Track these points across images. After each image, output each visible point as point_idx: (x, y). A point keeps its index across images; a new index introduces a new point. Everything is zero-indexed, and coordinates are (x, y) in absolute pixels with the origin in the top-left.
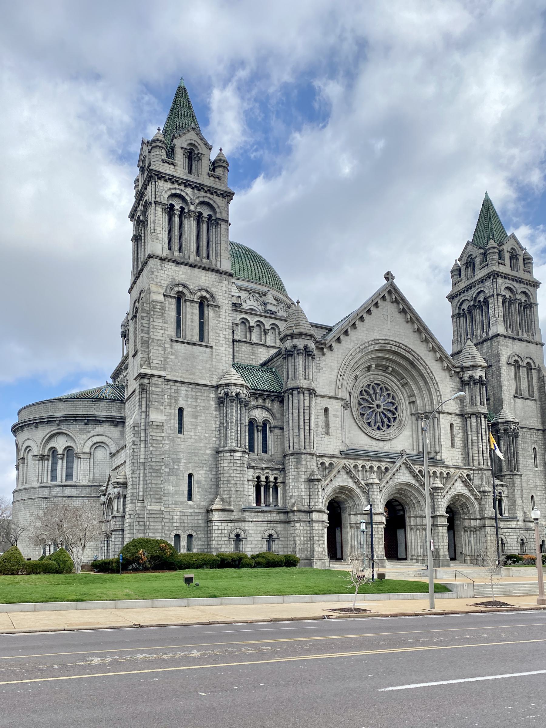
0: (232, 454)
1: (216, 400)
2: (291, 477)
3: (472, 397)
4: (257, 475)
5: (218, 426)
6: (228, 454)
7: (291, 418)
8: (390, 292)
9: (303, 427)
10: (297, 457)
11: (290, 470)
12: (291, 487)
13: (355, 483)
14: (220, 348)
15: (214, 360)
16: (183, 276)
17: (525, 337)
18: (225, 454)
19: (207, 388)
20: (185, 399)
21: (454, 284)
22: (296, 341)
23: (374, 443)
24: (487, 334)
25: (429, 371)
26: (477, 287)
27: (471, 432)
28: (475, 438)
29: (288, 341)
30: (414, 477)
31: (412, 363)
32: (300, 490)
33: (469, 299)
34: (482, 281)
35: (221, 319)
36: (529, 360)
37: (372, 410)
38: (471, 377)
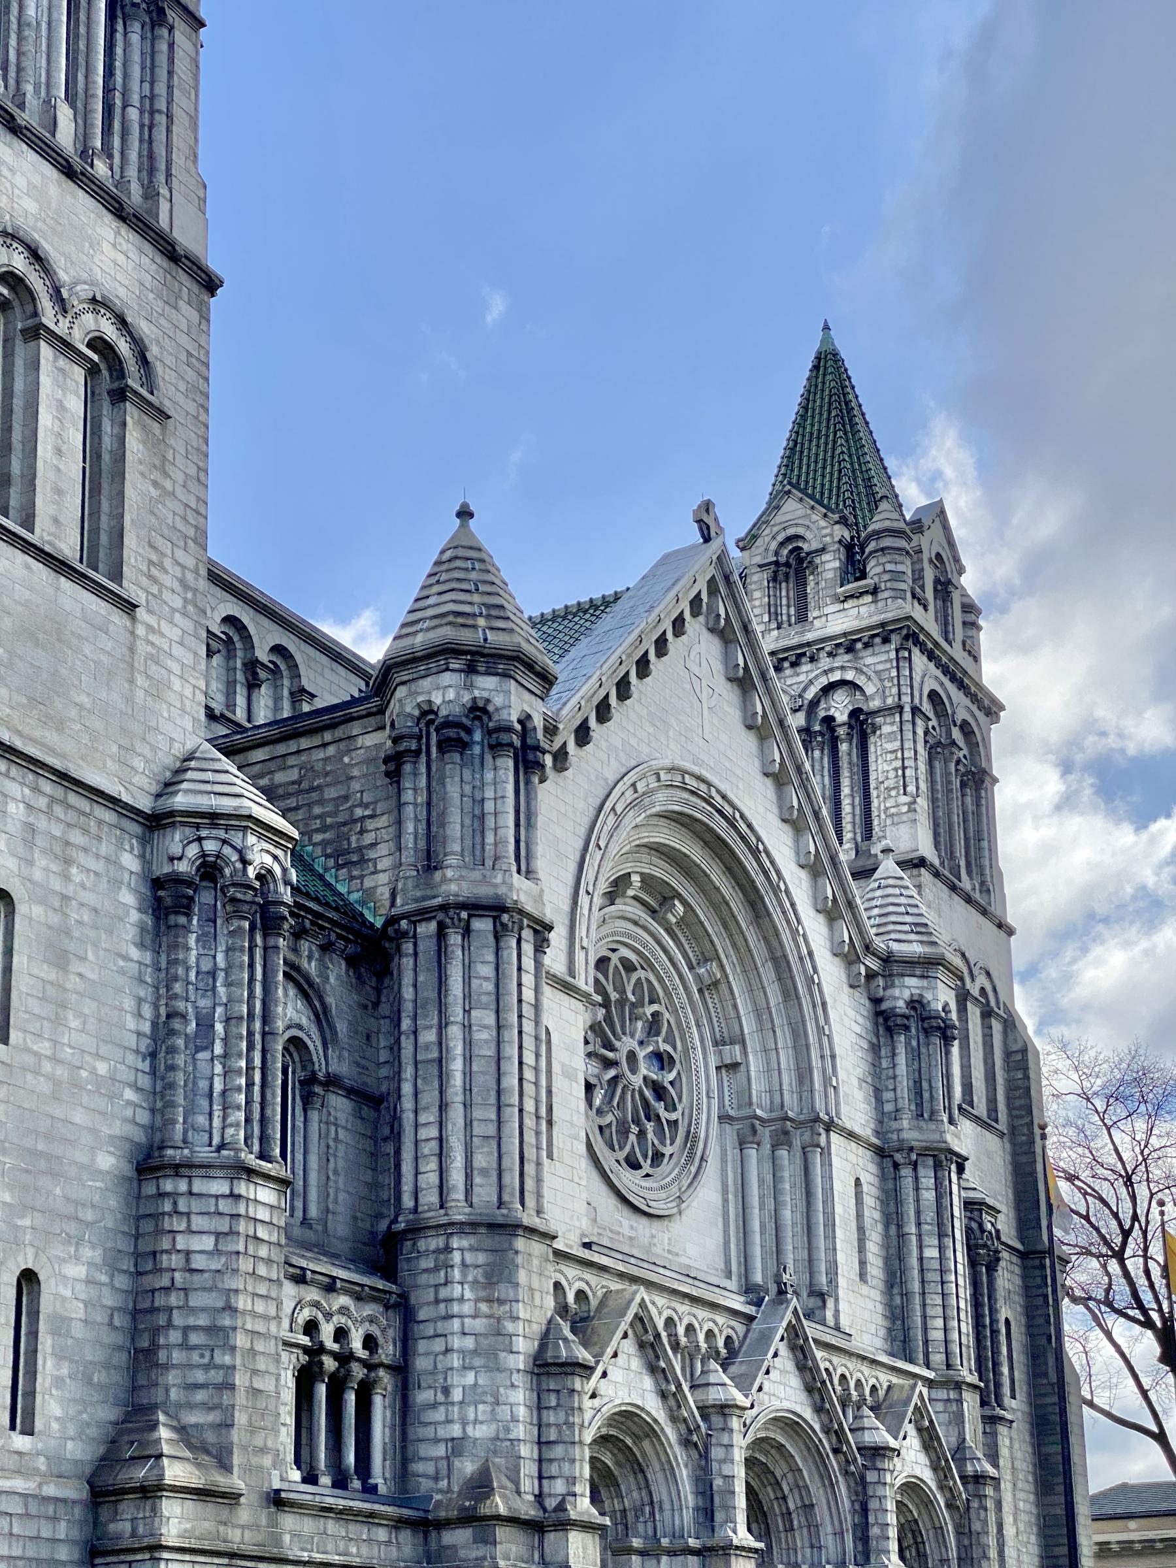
0: (242, 1188)
1: (145, 890)
2: (456, 1342)
4: (305, 1315)
5: (146, 1028)
6: (220, 1187)
7: (457, 1048)
9: (515, 1100)
10: (488, 1241)
11: (456, 1308)
12: (457, 1395)
13: (663, 1395)
14: (165, 628)
15: (140, 680)
16: (31, 206)
18: (198, 1186)
19: (109, 816)
20: (20, 850)
22: (486, 685)
23: (626, 1222)
25: (804, 951)
27: (919, 1224)
28: (931, 1253)
29: (447, 678)
30: (809, 1389)
32: (504, 1412)
35: (168, 485)
37: (612, 1073)
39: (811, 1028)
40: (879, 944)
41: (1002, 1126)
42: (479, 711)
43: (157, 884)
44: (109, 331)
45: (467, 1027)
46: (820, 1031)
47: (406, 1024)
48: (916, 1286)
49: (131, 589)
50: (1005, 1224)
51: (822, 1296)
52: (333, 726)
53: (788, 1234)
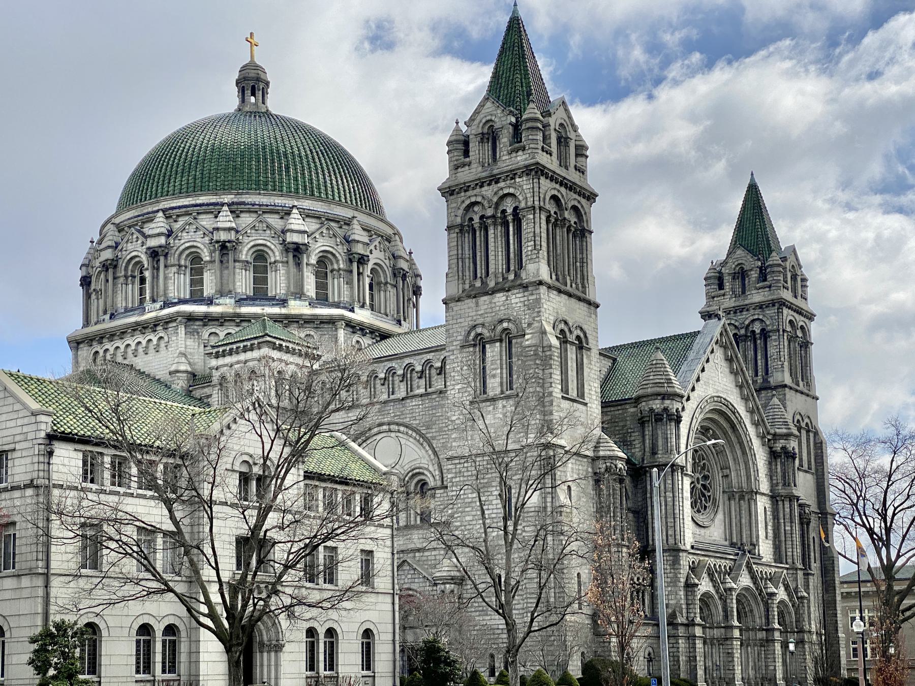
3: (784, 474)
8: (721, 334)
16: (564, 309)
17: (801, 387)
21: (711, 297)
24: (765, 380)
26: (752, 311)
28: (788, 528)
29: (657, 402)
31: (733, 427)
33: (737, 324)
34: (761, 306)
36: (806, 420)
38: (784, 448)
39: (750, 462)
40: (772, 431)
41: (813, 471)
42: (666, 409)
43: (595, 473)
44: (582, 335)
45: (665, 497)
46: (753, 463)
47: (648, 495)
48: (783, 539)
49: (587, 400)
50: (814, 508)
51: (754, 545)
52: (621, 405)
53: (744, 526)
